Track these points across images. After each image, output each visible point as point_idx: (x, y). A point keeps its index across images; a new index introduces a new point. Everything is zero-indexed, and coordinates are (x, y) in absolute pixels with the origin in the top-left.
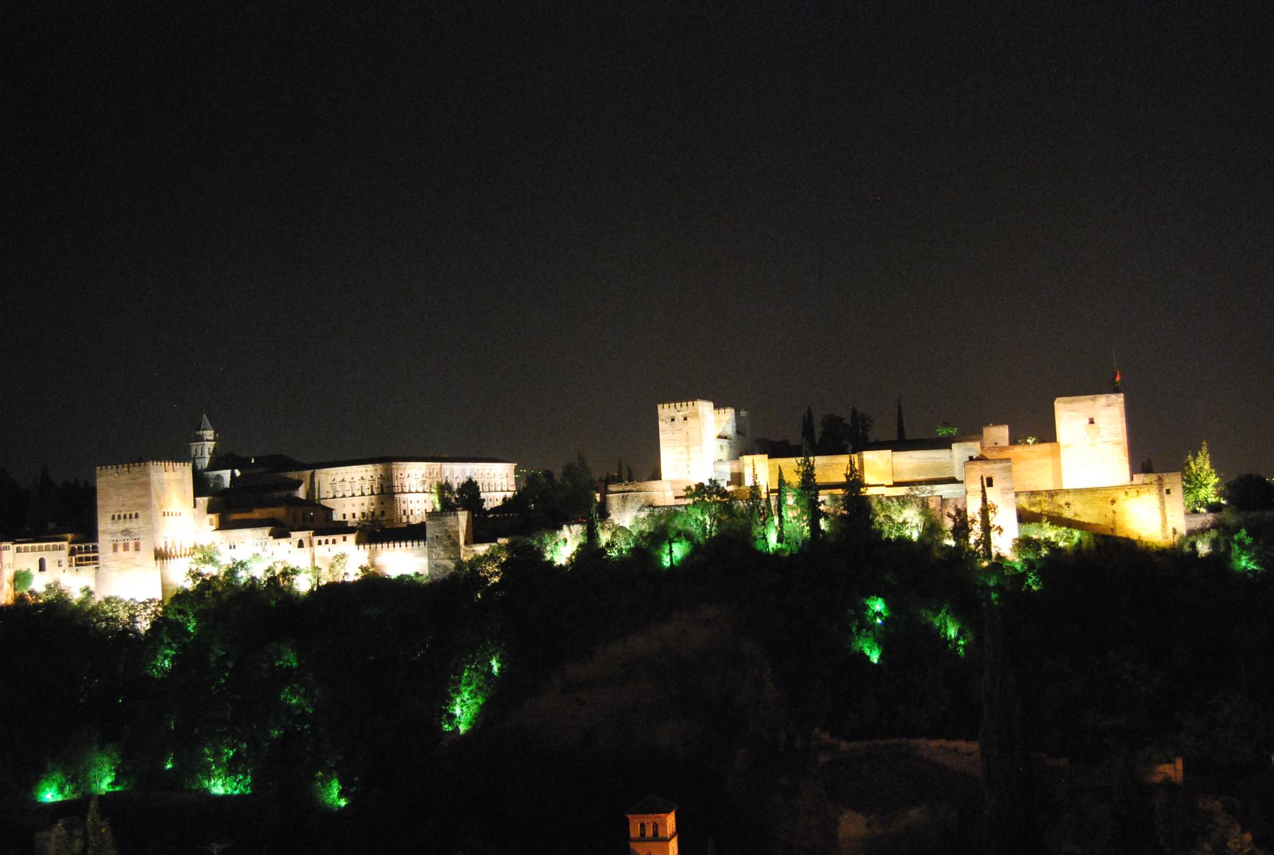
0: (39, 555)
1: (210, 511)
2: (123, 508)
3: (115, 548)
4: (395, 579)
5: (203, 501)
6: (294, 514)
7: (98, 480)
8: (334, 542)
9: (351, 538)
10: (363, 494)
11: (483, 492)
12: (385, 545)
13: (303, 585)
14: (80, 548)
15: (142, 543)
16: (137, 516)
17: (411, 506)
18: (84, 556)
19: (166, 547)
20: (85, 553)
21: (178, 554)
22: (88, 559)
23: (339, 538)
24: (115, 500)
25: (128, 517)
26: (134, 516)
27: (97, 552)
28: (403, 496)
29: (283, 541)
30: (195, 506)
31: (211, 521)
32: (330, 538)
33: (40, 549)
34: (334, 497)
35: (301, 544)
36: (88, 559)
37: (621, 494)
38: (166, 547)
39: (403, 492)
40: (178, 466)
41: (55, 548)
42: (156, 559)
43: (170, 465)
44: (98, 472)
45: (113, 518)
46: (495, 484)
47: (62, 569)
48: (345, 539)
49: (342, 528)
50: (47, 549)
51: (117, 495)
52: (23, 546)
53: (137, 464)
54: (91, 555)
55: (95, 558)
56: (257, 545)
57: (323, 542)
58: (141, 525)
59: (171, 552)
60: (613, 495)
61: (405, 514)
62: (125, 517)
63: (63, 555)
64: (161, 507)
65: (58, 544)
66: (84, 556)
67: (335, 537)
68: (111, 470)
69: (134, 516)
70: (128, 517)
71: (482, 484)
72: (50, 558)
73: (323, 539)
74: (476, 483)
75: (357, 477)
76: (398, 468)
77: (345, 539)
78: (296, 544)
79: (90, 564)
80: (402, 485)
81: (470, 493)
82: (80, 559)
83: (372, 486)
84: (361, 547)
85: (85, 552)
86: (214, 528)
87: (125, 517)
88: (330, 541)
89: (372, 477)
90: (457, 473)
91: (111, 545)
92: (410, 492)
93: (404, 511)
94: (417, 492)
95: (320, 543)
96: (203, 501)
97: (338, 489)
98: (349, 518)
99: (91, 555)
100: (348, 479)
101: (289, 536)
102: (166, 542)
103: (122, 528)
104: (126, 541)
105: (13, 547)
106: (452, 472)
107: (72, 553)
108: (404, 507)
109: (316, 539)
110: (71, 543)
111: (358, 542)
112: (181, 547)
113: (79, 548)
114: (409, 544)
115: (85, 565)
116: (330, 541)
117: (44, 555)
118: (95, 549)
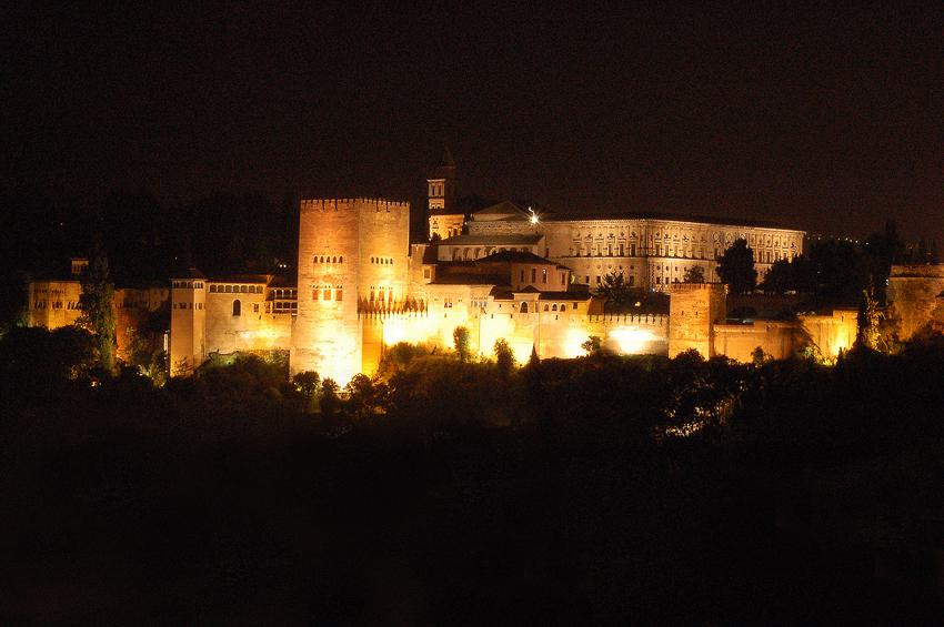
0: (234, 297)
1: (426, 261)
2: (327, 250)
3: (315, 298)
4: (626, 356)
5: (420, 248)
6: (523, 273)
7: (302, 215)
8: (563, 309)
9: (584, 305)
10: (611, 255)
11: (760, 262)
12: (622, 318)
13: (521, 358)
14: (279, 292)
15: (345, 292)
16: (341, 261)
17: (666, 274)
18: (283, 301)
19: (372, 299)
20: (286, 298)
21: (387, 307)
22: (287, 305)
23: (569, 304)
24: (318, 240)
25: (331, 260)
26: (338, 260)
27: (296, 299)
28: (660, 260)
29: (506, 304)
30: (410, 255)
31: (427, 272)
32: (559, 304)
33: (236, 290)
34: (578, 256)
35: (524, 309)
36: (287, 305)
37: (904, 279)
38: (372, 299)
39: (658, 256)
40: (392, 205)
41: (252, 290)
42: (359, 312)
43: (382, 204)
44: (302, 207)
45: (316, 260)
46: (776, 254)
47: (257, 315)
48: (575, 306)
49: (576, 293)
50: (244, 290)
51: (322, 234)
52: (217, 285)
53: (345, 200)
54: (291, 302)
55: (295, 305)
56: (476, 305)
57: (551, 308)
58: (346, 271)
59: (378, 304)
60: (897, 279)
61: (658, 283)
62: (328, 261)
63: (260, 299)
64: (372, 251)
65: (256, 285)
66: (283, 301)
67: (565, 303)
68: (316, 204)
69: (338, 260)
70: (331, 260)
71: (760, 254)
72: (247, 301)
73: (551, 304)
74: (750, 252)
75: (606, 234)
76: (653, 227)
77: (575, 306)
78: (519, 307)
79: (288, 312)
80: (657, 246)
81: (736, 263)
82: (279, 305)
83: (622, 246)
84: (594, 317)
85: (285, 299)
86: (429, 281)
87: (328, 261)
88: (559, 308)
89: (622, 235)
90: (731, 233)
91: (311, 292)
92: (667, 256)
93: (658, 279)
94: (676, 257)
95: (547, 310)
96: (420, 248)
97: (583, 246)
98: (593, 284)
99: (291, 302)
100: (596, 233)
101: (512, 297)
102: (372, 294)
103: (324, 273)
104: (328, 289)
105: (207, 286)
106: (722, 237)
107: (270, 297)
108: (657, 273)
109: (543, 304)
110: (269, 286)
111: (591, 312)
112: (390, 299)
113: (279, 292)
114: (650, 318)
115: (285, 312)
116: (559, 308)
117: (240, 297)
118: (295, 292)
